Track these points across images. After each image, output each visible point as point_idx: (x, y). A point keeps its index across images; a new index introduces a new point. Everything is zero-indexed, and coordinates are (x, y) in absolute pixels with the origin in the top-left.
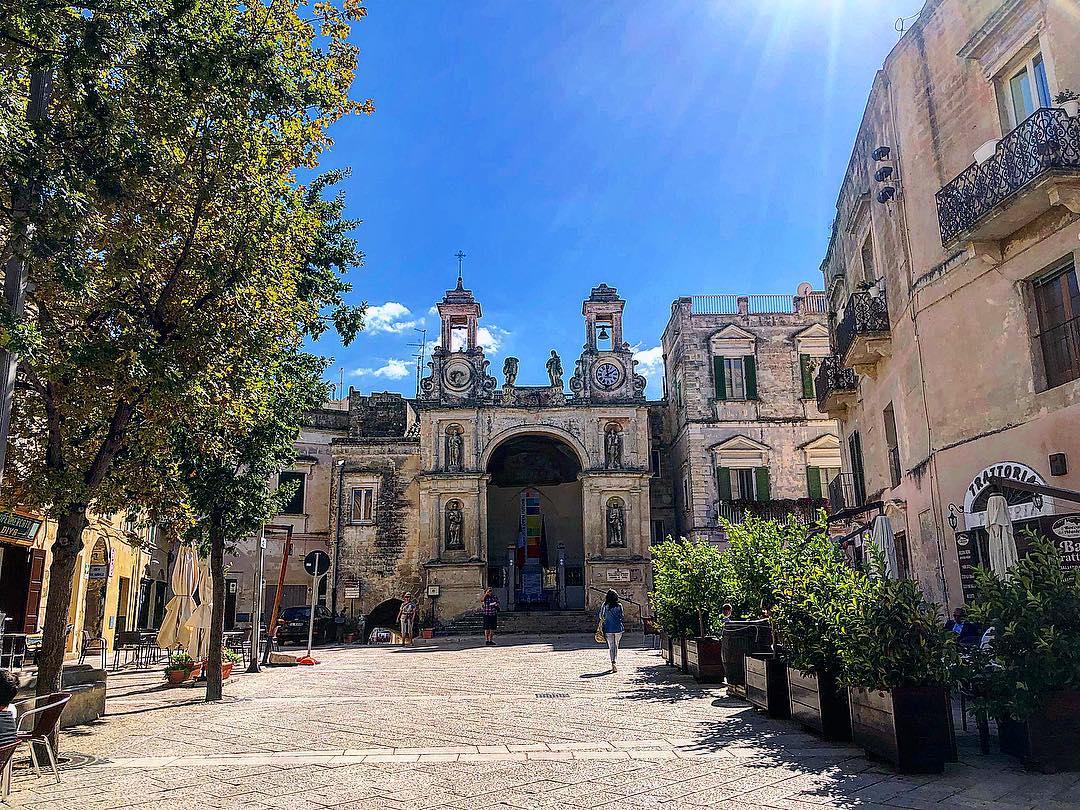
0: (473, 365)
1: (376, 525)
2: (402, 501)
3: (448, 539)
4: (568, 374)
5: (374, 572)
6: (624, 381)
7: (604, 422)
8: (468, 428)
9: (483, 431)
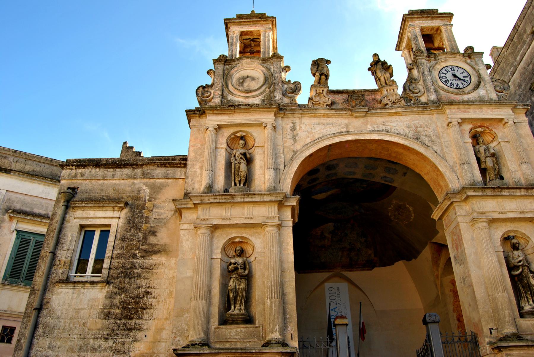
0: (269, 70)
1: (108, 282)
2: (152, 245)
3: (227, 303)
4: (400, 76)
6: (479, 83)
7: (467, 127)
8: (260, 137)
9: (285, 140)
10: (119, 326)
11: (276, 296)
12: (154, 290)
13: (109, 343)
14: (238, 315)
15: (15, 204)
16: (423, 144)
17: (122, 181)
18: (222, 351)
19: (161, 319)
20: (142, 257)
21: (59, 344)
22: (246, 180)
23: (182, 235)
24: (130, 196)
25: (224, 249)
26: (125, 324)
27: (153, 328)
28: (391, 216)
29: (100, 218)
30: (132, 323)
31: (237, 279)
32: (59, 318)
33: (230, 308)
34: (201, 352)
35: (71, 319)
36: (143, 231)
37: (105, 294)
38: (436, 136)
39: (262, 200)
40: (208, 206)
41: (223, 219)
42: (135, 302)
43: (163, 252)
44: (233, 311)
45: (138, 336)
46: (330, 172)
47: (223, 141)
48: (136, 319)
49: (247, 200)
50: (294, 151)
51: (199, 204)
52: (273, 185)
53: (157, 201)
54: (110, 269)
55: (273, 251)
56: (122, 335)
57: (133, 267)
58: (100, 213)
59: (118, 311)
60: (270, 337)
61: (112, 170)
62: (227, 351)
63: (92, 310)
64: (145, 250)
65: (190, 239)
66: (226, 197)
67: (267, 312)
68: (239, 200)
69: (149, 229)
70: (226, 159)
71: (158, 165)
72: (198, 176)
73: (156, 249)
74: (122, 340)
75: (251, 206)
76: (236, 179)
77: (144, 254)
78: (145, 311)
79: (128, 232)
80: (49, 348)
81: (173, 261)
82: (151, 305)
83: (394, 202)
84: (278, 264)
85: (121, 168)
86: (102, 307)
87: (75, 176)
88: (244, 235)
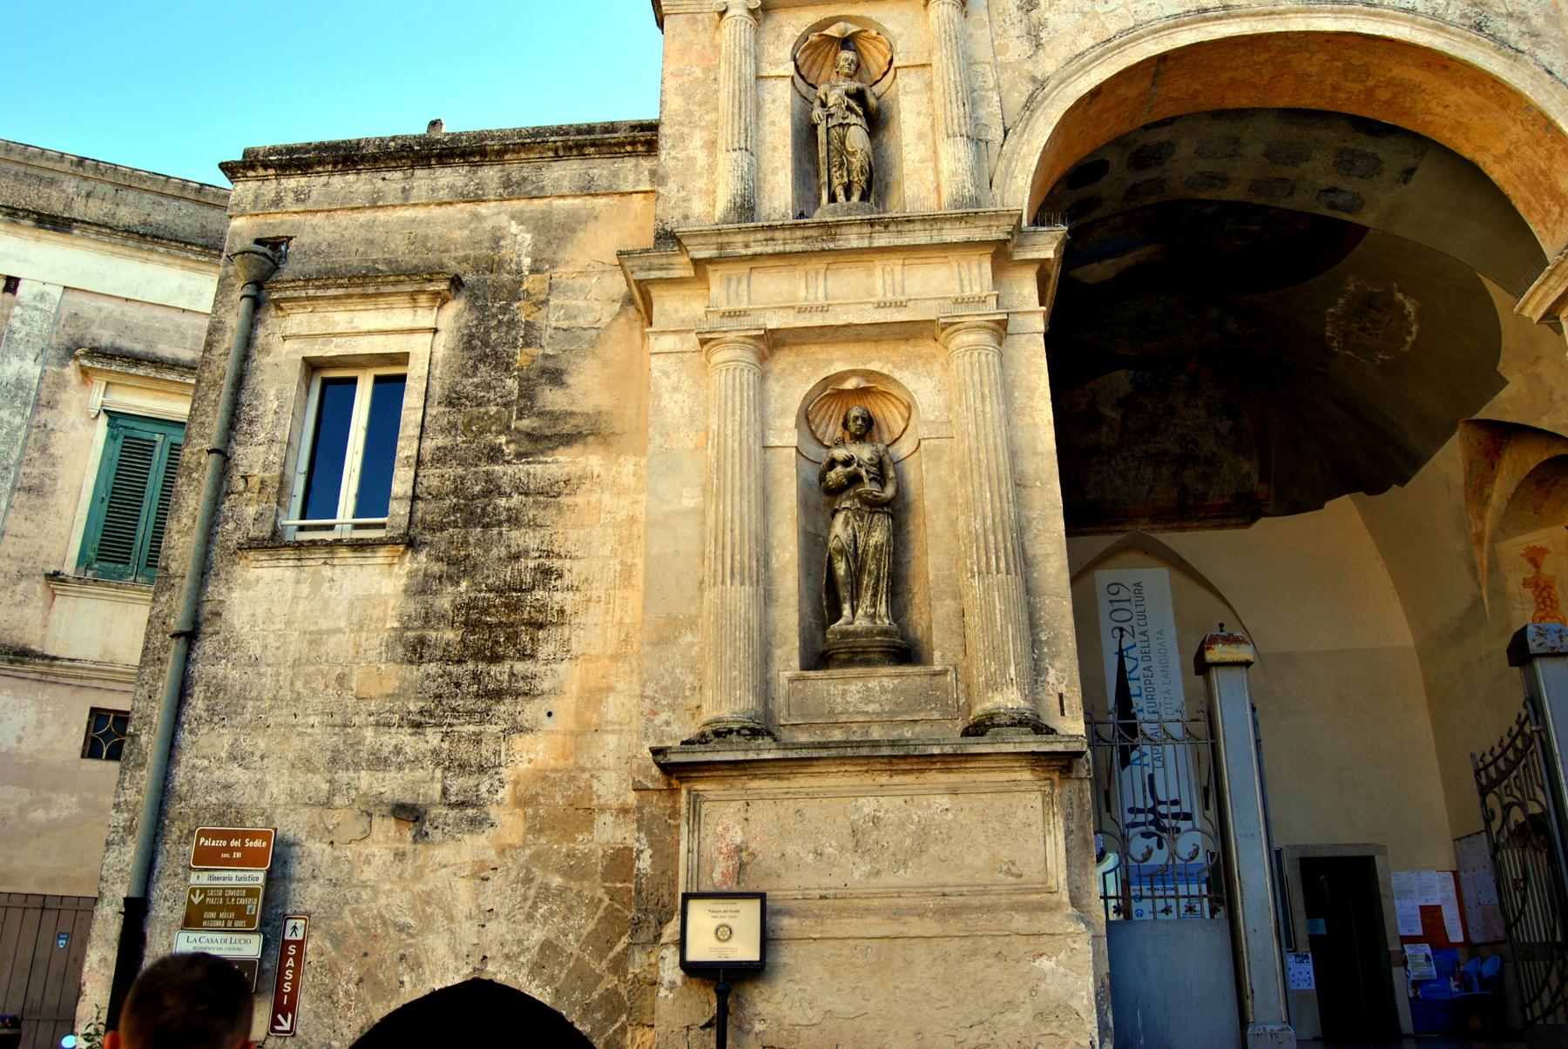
2: (555, 417)
3: (826, 595)
5: (369, 809)
10: (458, 685)
11: (1002, 565)
12: (568, 563)
13: (429, 738)
14: (868, 633)
15: (95, 331)
16: (1500, 44)
17: (436, 211)
18: (824, 753)
19: (598, 658)
20: (519, 456)
21: (262, 744)
22: (869, 182)
23: (655, 373)
24: (466, 259)
25: (806, 418)
26: (476, 677)
27: (573, 688)
28: (1332, 339)
29: (369, 333)
30: (500, 672)
31: (857, 513)
32: (255, 662)
33: (836, 614)
34: (751, 756)
35: (297, 663)
36: (520, 369)
37: (404, 581)
38: (1547, 16)
39: (936, 240)
40: (742, 269)
41: (801, 310)
42: (506, 605)
43: (590, 439)
44: (852, 623)
45: (523, 716)
46: (1143, 176)
47: (781, 55)
48: (512, 658)
49: (882, 240)
50: (1034, 79)
51: (710, 261)
52: (970, 190)
53: (560, 270)
54: (415, 498)
55: (981, 417)
56: (471, 713)
57: (493, 489)
58: (369, 318)
59: (450, 635)
60: (988, 705)
61: (398, 175)
62: (842, 752)
63: (364, 635)
64: (528, 435)
65: (686, 384)
66: (807, 233)
67: (973, 620)
68: (855, 244)
69: (540, 362)
70: (793, 116)
71: (556, 150)
72: (700, 175)
73: (567, 428)
74: (472, 728)
75: (895, 263)
76: (836, 182)
77: (526, 446)
78: (541, 634)
79: (466, 375)
80: (233, 758)
81: (627, 468)
82: (562, 612)
83: (1352, 287)
84: (1003, 457)
85: (429, 166)
86: (396, 625)
87: (278, 201)
88: (874, 366)
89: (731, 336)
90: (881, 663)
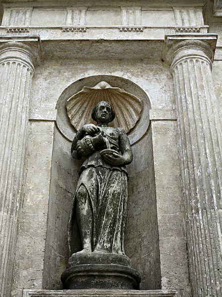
14: (105, 259)
25: (64, 107)
31: (98, 168)
41: (66, 30)
88: (118, 74)
89: (14, 41)
90: (116, 287)
